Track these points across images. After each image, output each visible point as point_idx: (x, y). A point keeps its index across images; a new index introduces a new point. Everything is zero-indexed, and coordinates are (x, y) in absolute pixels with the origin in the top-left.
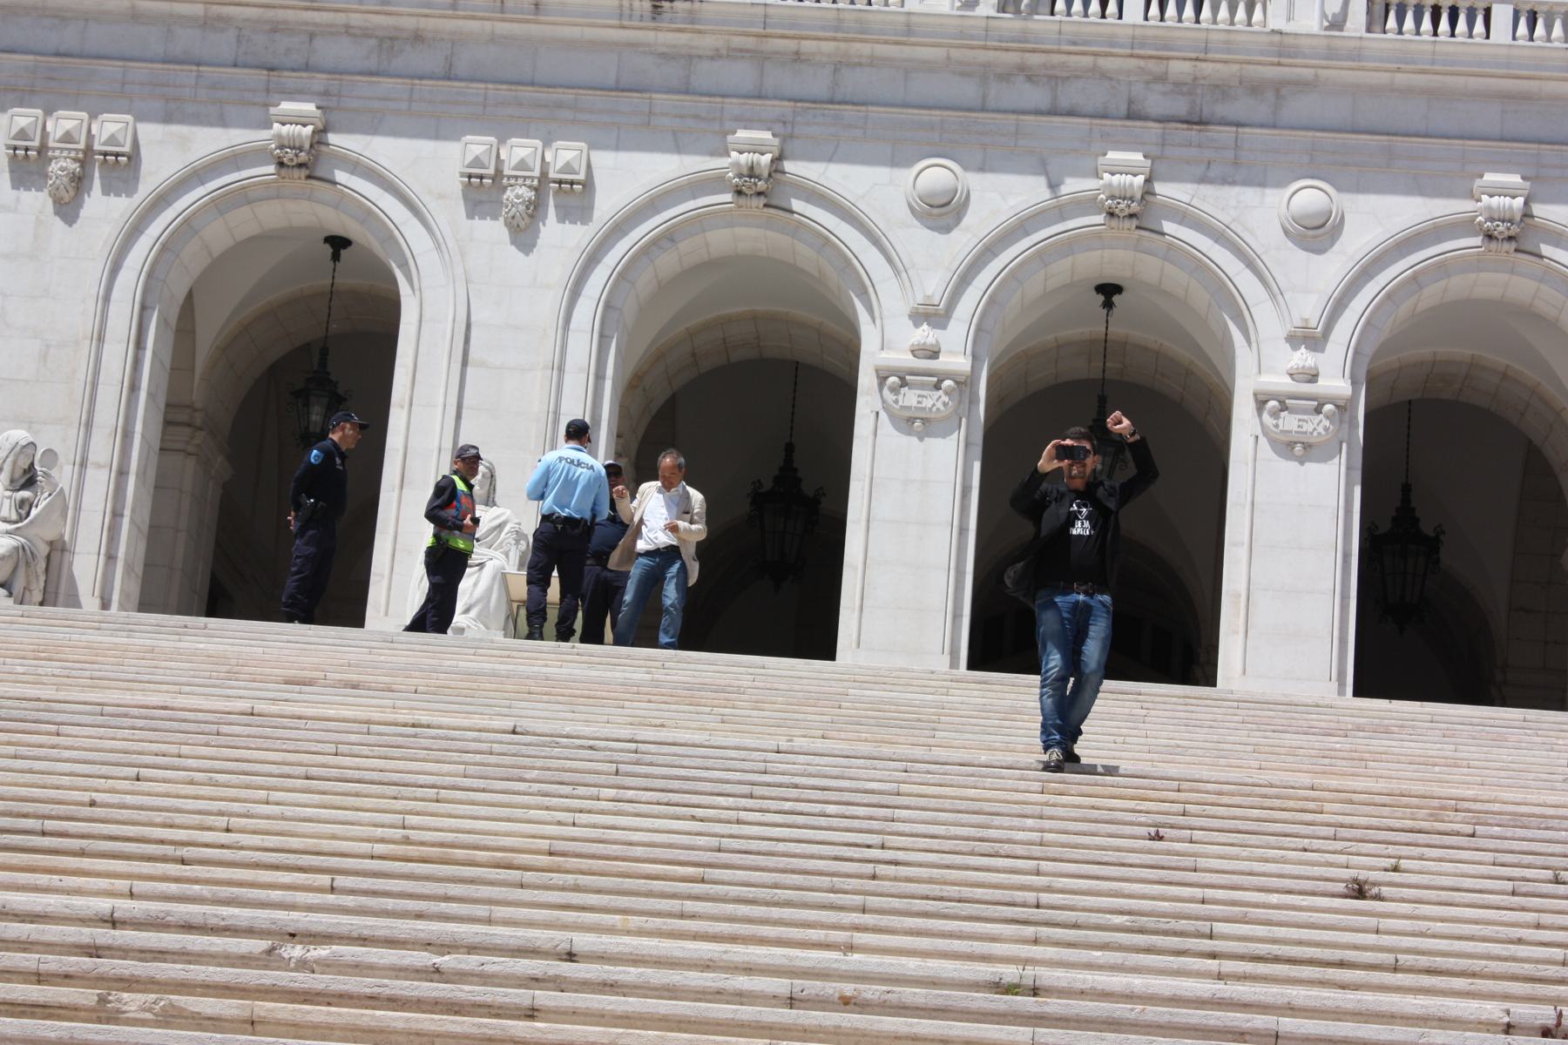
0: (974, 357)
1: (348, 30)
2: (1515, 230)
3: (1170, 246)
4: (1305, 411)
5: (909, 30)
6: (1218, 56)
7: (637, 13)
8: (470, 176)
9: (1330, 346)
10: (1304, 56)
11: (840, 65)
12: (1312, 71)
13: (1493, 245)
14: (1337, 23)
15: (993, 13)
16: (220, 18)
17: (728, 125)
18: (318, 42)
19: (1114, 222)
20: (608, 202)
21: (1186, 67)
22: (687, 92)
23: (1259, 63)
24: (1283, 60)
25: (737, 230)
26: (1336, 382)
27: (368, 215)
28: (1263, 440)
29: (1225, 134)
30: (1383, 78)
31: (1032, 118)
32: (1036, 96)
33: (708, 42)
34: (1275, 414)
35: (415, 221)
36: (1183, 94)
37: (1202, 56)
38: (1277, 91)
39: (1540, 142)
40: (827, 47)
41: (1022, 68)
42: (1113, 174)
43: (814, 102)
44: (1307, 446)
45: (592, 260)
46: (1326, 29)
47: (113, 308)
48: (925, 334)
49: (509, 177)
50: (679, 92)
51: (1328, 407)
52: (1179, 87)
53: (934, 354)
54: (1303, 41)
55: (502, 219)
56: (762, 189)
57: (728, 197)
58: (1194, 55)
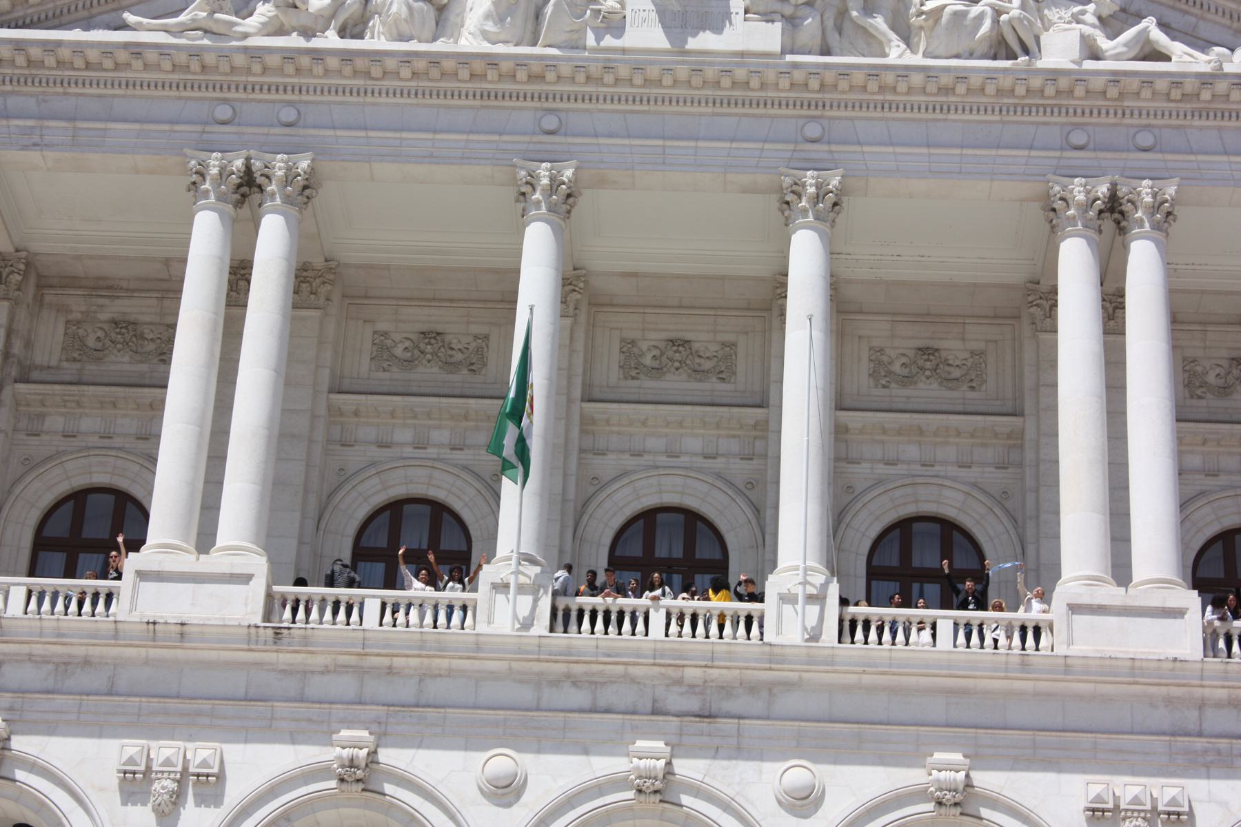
1: (30, 658)
2: (959, 797)
3: (688, 816)
5: (478, 647)
6: (722, 664)
7: (262, 639)
8: (125, 773)
10: (790, 663)
11: (424, 676)
12: (797, 674)
13: (943, 810)
14: (815, 636)
15: (546, 633)
18: (6, 668)
19: (642, 797)
22: (302, 701)
23: (755, 669)
24: (774, 666)
30: (852, 678)
31: (577, 715)
32: (580, 698)
33: (319, 660)
35: (80, 810)
36: (695, 693)
37: (709, 664)
38: (770, 690)
39: (976, 727)
40: (414, 662)
41: (568, 676)
42: (640, 759)
43: (403, 706)
46: (807, 641)
49: (157, 772)
50: (295, 701)
54: (788, 651)
55: (150, 805)
57: (333, 783)
58: (703, 663)
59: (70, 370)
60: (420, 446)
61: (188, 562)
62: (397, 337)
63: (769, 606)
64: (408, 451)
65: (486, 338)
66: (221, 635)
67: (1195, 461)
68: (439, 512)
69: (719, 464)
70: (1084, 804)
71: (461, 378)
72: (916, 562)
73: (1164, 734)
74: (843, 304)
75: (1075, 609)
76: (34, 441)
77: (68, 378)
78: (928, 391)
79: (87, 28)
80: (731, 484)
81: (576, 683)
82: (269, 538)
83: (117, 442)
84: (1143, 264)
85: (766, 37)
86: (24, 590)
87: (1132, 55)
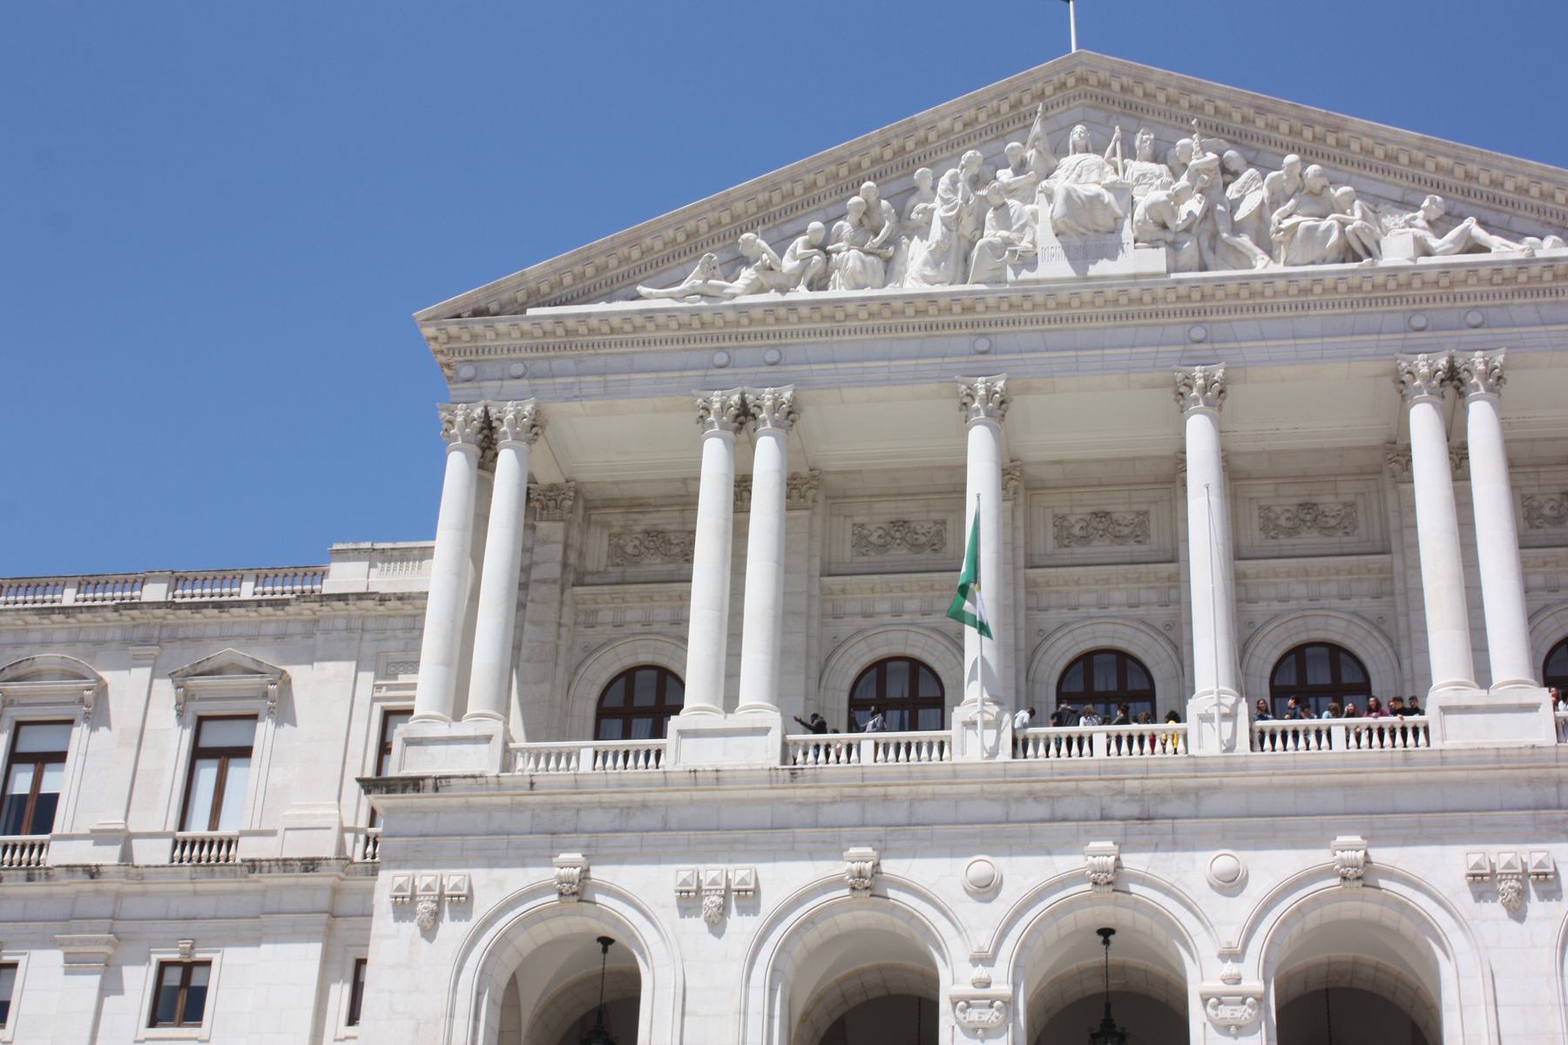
0: (1015, 985)
1: (600, 805)
2: (1360, 872)
3: (1137, 901)
4: (1234, 1004)
5: (955, 775)
9: (1247, 958)
11: (913, 801)
13: (1348, 883)
14: (1230, 748)
15: (1009, 759)
16: (520, 804)
17: (844, 845)
20: (770, 902)
21: (1136, 783)
25: (856, 913)
26: (1253, 982)
27: (618, 922)
28: (1209, 1025)
29: (1165, 825)
30: (1265, 780)
31: (1038, 825)
32: (1041, 810)
33: (829, 793)
34: (1215, 1007)
35: (648, 924)
39: (1371, 813)
40: (904, 790)
41: (1030, 793)
44: (1239, 1027)
45: (762, 940)
47: (459, 996)
48: (981, 972)
51: (1250, 1000)
52: (1133, 797)
53: (987, 985)
56: (869, 885)
57: (847, 891)
59: (615, 573)
60: (896, 613)
61: (718, 720)
62: (872, 527)
63: (1191, 723)
64: (887, 619)
65: (944, 522)
66: (748, 778)
67: (1538, 580)
68: (916, 667)
69: (1141, 611)
70: (1465, 871)
71: (927, 555)
72: (1311, 681)
73: (1528, 808)
74: (1235, 475)
75: (1446, 710)
76: (590, 631)
77: (613, 580)
78: (1310, 538)
79: (610, 301)
80: (1153, 628)
81: (1036, 798)
82: (779, 696)
83: (656, 628)
84: (1481, 420)
85: (1154, 260)
86: (591, 752)
87: (1459, 248)
